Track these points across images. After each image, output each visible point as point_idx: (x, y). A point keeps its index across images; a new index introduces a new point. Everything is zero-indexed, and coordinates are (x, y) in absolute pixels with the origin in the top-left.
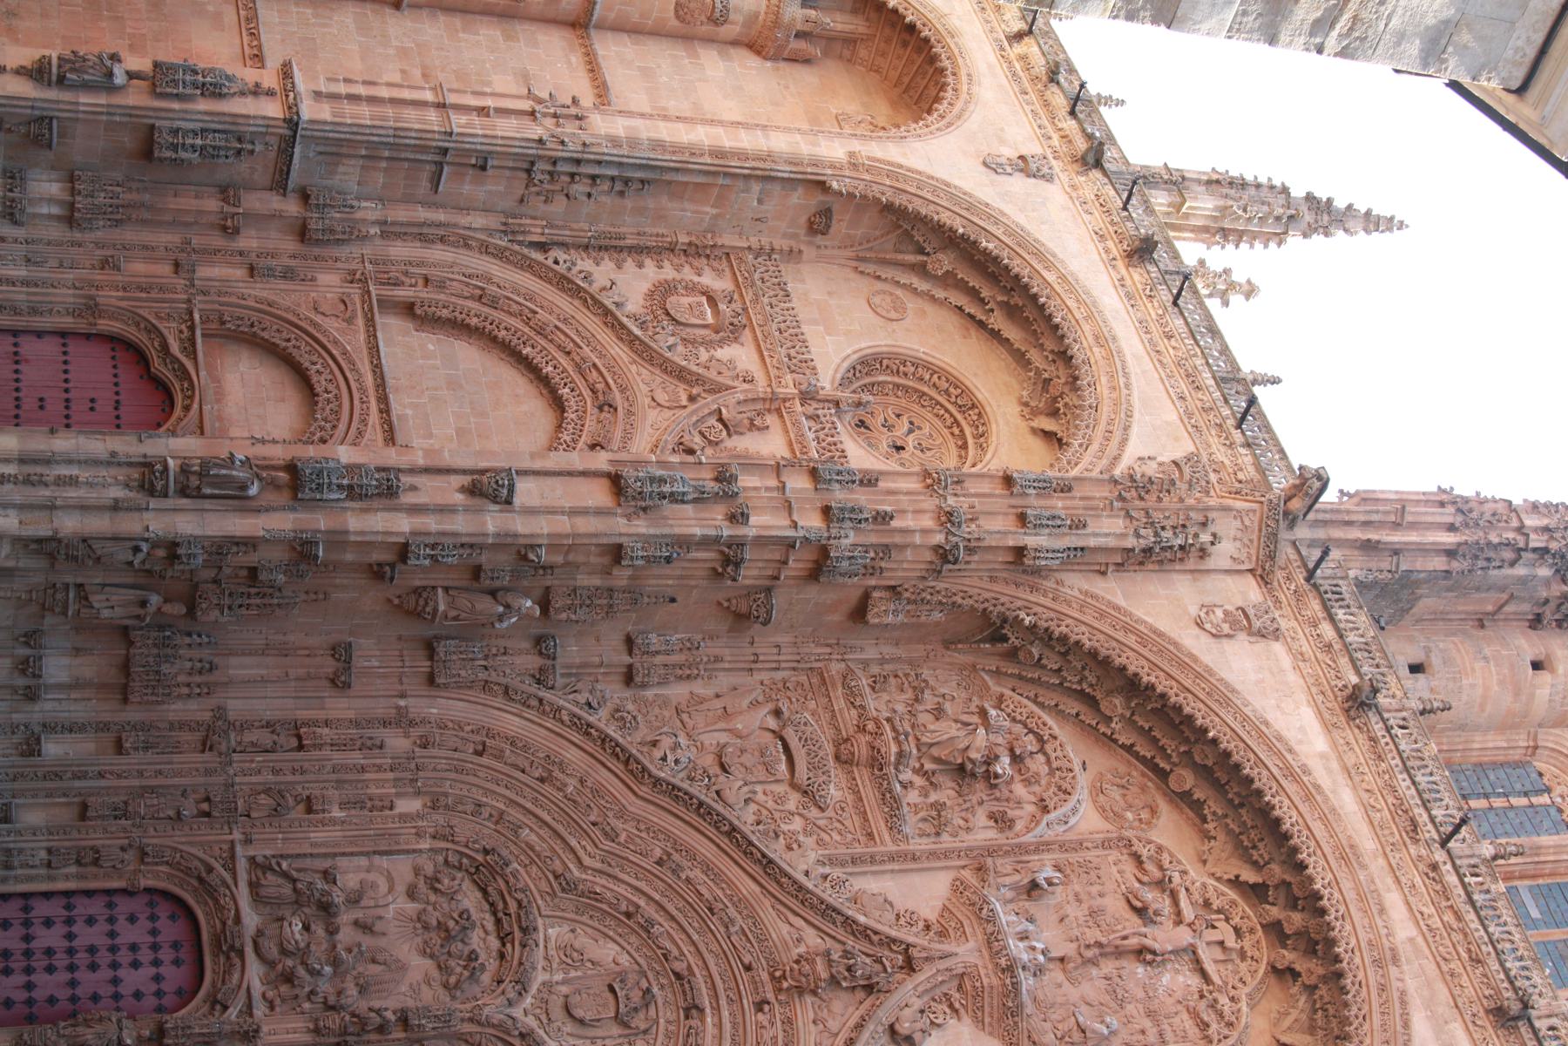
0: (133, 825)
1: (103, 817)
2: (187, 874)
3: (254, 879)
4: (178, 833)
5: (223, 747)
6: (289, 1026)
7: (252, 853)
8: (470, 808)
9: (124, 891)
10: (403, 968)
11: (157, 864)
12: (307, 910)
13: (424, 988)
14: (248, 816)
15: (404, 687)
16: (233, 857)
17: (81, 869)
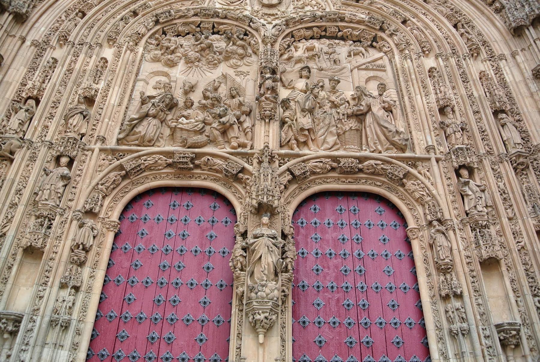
0: (62, 215)
1: (46, 236)
2: (118, 185)
3: (137, 142)
4: (79, 186)
5: (16, 143)
6: (263, 134)
7: (115, 140)
8: (122, 23)
9: (116, 236)
10: (225, 76)
11: (102, 205)
12: (170, 117)
13: (239, 70)
14: (83, 135)
15: (18, 36)
16: (113, 151)
17: (88, 264)
